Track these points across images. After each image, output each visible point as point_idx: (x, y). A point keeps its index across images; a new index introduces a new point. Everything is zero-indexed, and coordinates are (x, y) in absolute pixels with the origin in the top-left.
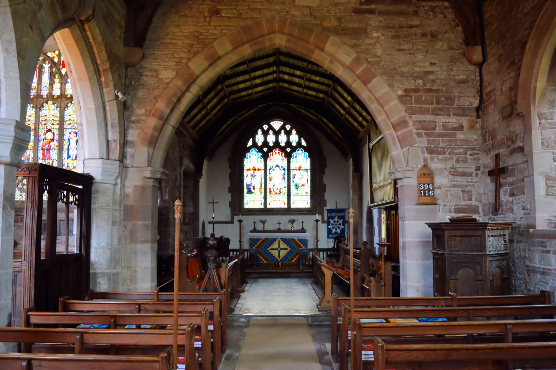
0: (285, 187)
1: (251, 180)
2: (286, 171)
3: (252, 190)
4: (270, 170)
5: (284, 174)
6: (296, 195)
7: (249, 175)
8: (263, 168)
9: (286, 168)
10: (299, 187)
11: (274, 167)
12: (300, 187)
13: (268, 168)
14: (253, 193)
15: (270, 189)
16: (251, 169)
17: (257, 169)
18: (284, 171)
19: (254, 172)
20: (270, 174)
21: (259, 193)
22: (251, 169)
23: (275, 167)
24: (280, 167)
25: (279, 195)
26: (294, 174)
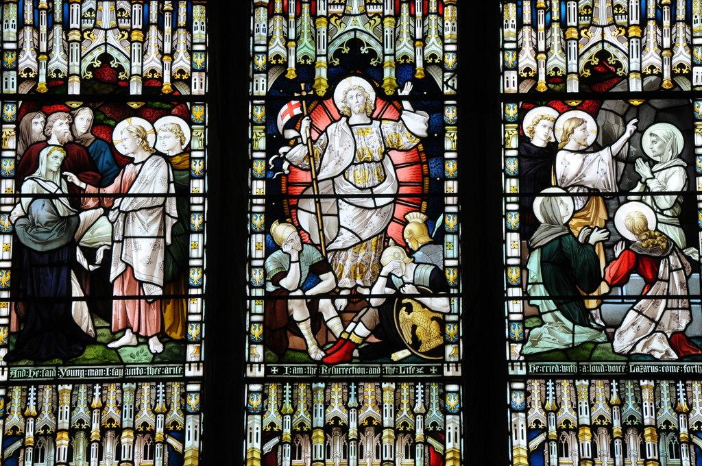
0: (438, 284)
1: (63, 206)
2: (450, 114)
3: (80, 312)
4: (273, 103)
5: (431, 144)
6: (571, 367)
7: (51, 159)
8: (199, 87)
9: (447, 84)
10: (597, 280)
11: (322, 73)
12: (604, 288)
13: (261, 85)
14: (91, 352)
15: (277, 300)
16: (74, 88)
17: (136, 89)
18: (417, 122)
19: (103, 127)
20: (276, 142)
21: (156, 346)
22: (74, 88)
23: (335, 78)
24: (388, 73)
25: (374, 370)
26: (539, 141)
